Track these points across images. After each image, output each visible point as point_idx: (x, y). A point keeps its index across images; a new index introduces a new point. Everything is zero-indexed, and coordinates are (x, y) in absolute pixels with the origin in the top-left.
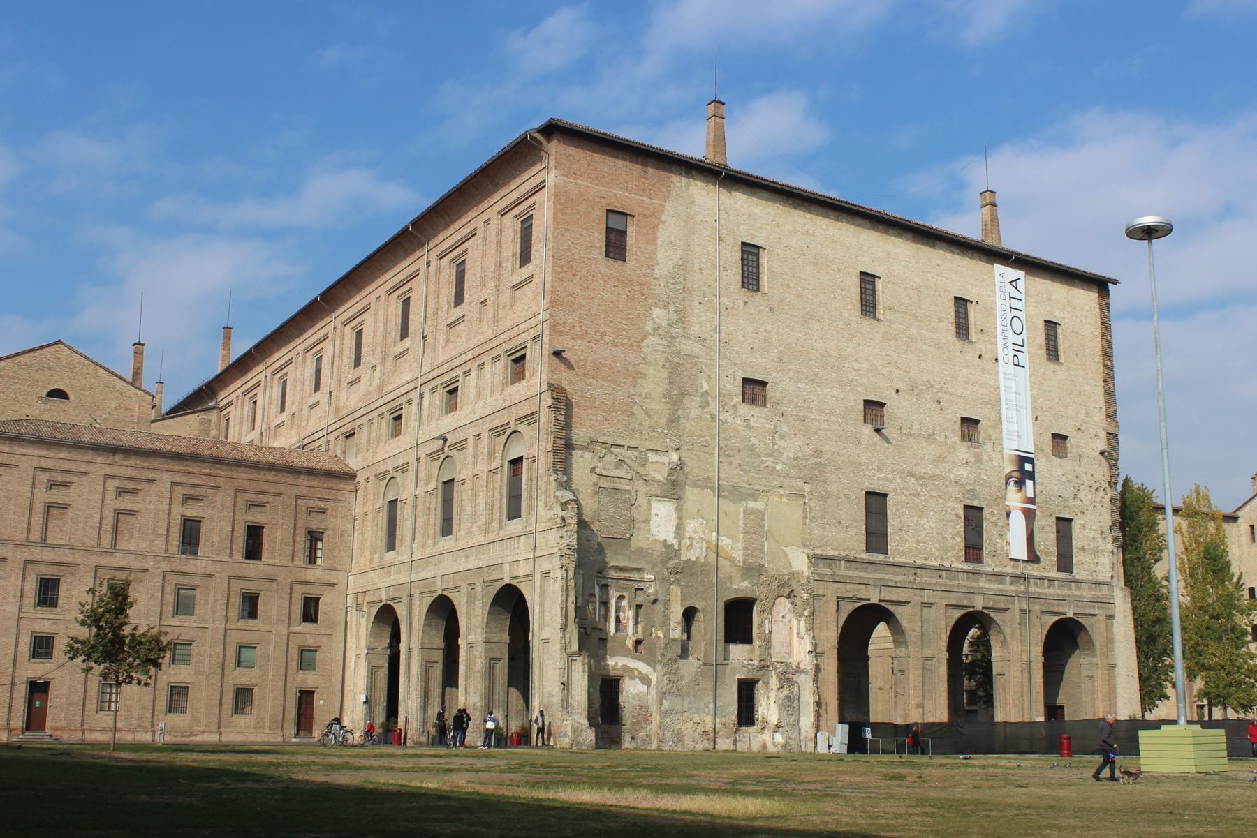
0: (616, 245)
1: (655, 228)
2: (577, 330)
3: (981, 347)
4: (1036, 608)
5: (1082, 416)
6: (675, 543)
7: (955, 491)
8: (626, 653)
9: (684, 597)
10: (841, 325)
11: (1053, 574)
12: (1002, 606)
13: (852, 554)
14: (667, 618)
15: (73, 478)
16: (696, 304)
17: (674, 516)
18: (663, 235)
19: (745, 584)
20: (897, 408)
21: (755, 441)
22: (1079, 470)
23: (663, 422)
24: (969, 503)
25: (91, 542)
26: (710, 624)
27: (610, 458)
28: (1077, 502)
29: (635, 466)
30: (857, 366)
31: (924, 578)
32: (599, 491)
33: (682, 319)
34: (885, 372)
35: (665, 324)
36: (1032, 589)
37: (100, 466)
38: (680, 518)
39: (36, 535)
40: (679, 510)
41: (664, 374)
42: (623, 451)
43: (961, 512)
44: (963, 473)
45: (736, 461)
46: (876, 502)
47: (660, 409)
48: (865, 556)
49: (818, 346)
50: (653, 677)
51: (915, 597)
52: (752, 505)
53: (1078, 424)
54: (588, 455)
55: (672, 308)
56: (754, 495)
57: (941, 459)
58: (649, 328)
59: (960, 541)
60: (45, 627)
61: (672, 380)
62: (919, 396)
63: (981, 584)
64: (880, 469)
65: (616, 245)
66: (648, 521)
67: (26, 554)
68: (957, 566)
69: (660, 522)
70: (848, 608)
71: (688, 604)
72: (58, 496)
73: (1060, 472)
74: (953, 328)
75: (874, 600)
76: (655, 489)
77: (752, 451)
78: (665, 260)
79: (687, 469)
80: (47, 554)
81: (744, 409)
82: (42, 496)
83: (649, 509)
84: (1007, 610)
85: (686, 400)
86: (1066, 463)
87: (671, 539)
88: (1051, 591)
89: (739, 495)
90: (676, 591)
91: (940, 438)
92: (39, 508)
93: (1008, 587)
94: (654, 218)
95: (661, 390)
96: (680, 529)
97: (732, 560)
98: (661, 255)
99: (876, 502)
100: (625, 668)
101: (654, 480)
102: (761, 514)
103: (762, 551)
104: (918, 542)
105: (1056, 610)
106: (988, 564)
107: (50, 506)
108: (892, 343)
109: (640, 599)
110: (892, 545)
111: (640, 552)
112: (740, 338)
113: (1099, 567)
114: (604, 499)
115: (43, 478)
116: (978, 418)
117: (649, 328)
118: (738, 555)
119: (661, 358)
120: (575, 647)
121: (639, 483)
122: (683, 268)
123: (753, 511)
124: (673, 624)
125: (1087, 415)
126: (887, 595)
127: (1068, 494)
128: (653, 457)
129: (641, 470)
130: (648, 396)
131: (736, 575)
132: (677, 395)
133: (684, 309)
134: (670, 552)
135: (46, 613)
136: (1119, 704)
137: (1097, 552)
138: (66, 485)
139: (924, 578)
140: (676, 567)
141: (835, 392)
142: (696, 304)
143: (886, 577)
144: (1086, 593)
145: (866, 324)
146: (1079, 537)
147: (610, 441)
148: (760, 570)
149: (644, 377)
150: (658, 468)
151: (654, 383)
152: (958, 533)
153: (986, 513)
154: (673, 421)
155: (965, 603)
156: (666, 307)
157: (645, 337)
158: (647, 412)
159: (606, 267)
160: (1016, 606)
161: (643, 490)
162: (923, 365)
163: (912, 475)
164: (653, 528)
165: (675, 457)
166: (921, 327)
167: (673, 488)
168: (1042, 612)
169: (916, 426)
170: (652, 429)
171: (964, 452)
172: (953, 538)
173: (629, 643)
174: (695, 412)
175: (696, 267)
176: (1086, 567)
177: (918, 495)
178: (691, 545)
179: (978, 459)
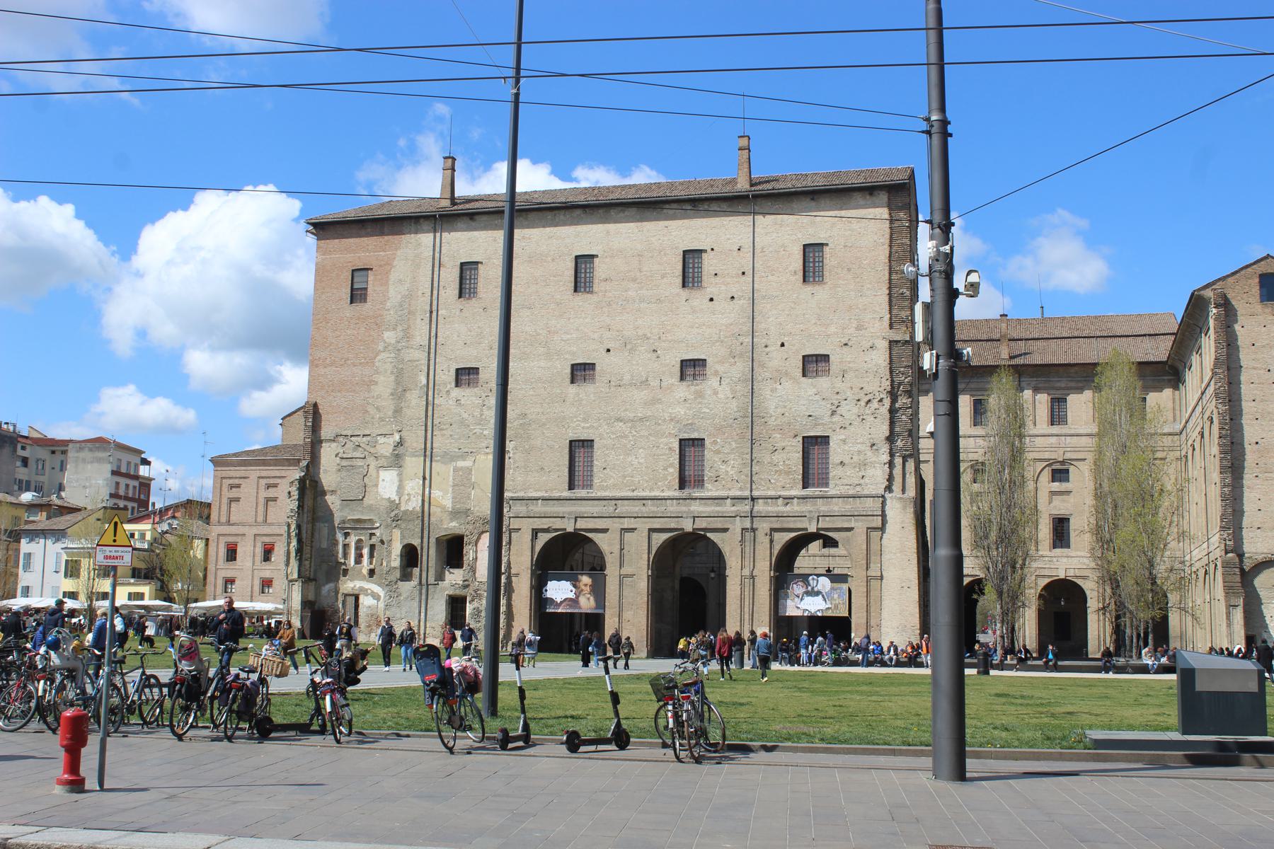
0: (357, 295)
1: (388, 273)
2: (328, 361)
3: (711, 286)
4: (763, 526)
5: (852, 330)
6: (397, 499)
7: (671, 428)
8: (363, 578)
9: (403, 537)
10: (553, 306)
11: (797, 491)
12: (720, 526)
13: (556, 494)
14: (390, 553)
15: (278, 481)
16: (419, 321)
17: (396, 479)
18: (394, 276)
19: (454, 524)
20: (604, 364)
21: (465, 416)
22: (839, 385)
23: (390, 413)
24: (686, 436)
25: (252, 520)
26: (430, 556)
27: (350, 445)
28: (836, 418)
29: (368, 448)
30: (565, 337)
31: (624, 508)
32: (341, 469)
33: (407, 335)
34: (596, 336)
35: (393, 341)
36: (760, 507)
37: (254, 472)
38: (400, 481)
39: (260, 519)
40: (400, 475)
41: (393, 378)
42: (359, 439)
43: (676, 446)
44: (680, 411)
45: (448, 433)
46: (579, 448)
47: (388, 405)
48: (567, 494)
49: (527, 329)
50: (382, 593)
51: (615, 525)
52: (461, 464)
53: (844, 340)
54: (334, 445)
55: (400, 328)
56: (464, 456)
57: (655, 401)
58: (381, 348)
59: (674, 472)
60: (267, 575)
61: (398, 383)
62: (632, 351)
63: (692, 508)
64: (585, 420)
65: (357, 295)
66: (377, 485)
67: (255, 530)
68: (667, 494)
69: (386, 485)
70: (543, 538)
71: (406, 542)
72: (234, 493)
73: (812, 391)
74: (680, 280)
75: (570, 529)
76: (382, 462)
77: (462, 422)
78: (395, 293)
79: (406, 445)
80: (233, 530)
81: (457, 392)
82: (264, 494)
83: (378, 477)
84: (726, 530)
85: (408, 394)
86: (823, 383)
87: (394, 497)
88: (788, 508)
89: (449, 458)
90: (397, 534)
91: (654, 383)
92: (262, 501)
93: (728, 508)
94: (389, 264)
95: (389, 391)
96: (401, 488)
97: (443, 508)
98: (392, 292)
99: (579, 448)
100: (361, 589)
101: (382, 456)
102: (469, 470)
103: (469, 498)
104: (625, 477)
105: (792, 526)
106: (710, 490)
107: (268, 500)
108: (605, 310)
109: (374, 540)
110: (596, 481)
111: (370, 508)
112: (455, 338)
113: (866, 480)
114: (344, 473)
115: (263, 482)
116: (703, 357)
117: (381, 348)
118: (448, 503)
119: (389, 367)
120: (295, 576)
121: (371, 461)
122: (410, 296)
123: (462, 468)
124: (393, 557)
125: (859, 328)
126: (581, 524)
127: (823, 410)
128: (381, 440)
129: (372, 450)
130: (379, 396)
131: (446, 517)
132: (400, 394)
133: (409, 327)
134: (393, 505)
135: (267, 565)
136: (885, 614)
137: (864, 465)
138: (238, 486)
139: (624, 508)
140: (397, 517)
141: (542, 364)
142: (419, 321)
143: (583, 509)
144: (837, 507)
145: (580, 297)
146: (836, 451)
147: (349, 433)
148: (467, 512)
149: (376, 383)
150: (386, 446)
151: (384, 385)
152: (671, 465)
153: (707, 442)
154: (398, 411)
155: (673, 526)
156: (394, 329)
157: (377, 354)
158: (378, 408)
159: (350, 311)
160: (737, 526)
161: (373, 463)
162: (640, 322)
163: (619, 420)
164: (380, 489)
165: (397, 437)
166: (641, 289)
167: (396, 460)
168: (773, 530)
169: (627, 377)
170: (382, 419)
171: (683, 390)
172: (665, 469)
173: (365, 571)
174: (414, 402)
175: (420, 293)
176: (845, 481)
177: (626, 437)
178: (409, 500)
179: (700, 395)
